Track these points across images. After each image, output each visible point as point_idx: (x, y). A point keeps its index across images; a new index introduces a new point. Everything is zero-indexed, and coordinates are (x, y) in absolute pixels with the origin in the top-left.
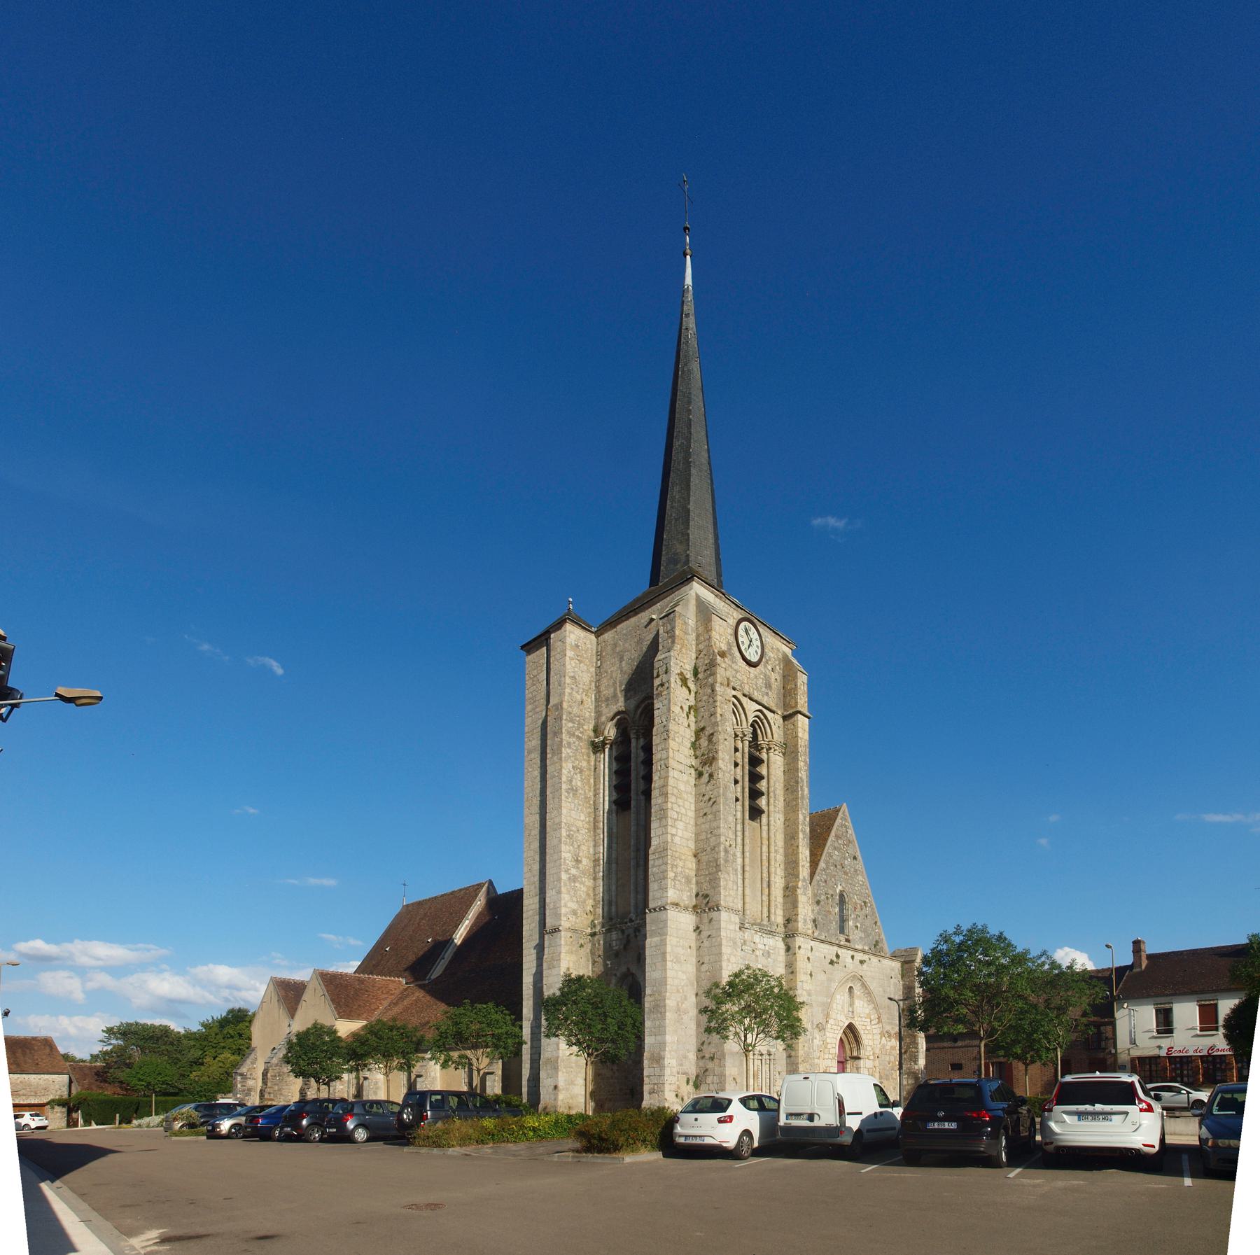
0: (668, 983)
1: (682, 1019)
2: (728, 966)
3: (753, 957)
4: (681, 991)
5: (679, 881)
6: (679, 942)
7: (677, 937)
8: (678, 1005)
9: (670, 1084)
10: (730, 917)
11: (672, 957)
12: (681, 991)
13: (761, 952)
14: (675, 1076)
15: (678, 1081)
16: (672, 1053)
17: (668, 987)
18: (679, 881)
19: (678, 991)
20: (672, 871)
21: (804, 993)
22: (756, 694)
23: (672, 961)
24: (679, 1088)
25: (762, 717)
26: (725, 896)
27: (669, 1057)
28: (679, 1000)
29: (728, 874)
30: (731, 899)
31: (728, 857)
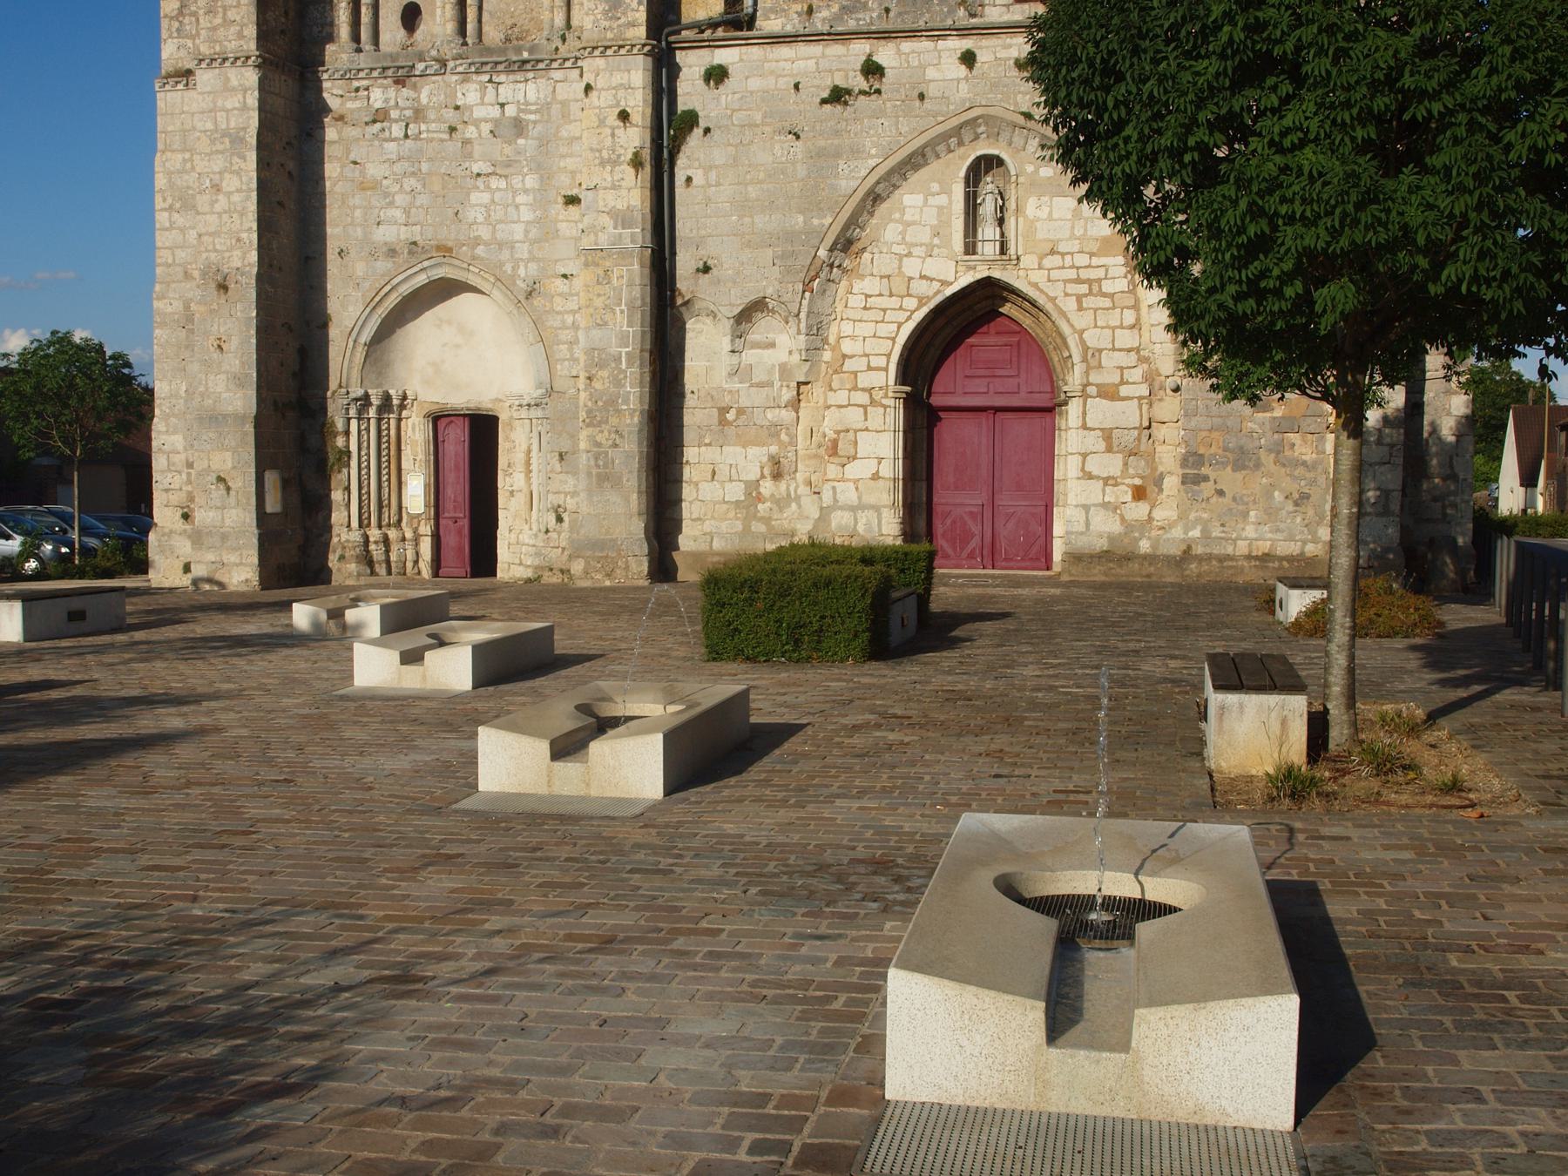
0: (159, 261)
2: (213, 203)
3: (453, 147)
7: (183, 151)
9: (167, 490)
10: (228, 79)
13: (486, 128)
14: (180, 472)
15: (189, 482)
16: (173, 420)
17: (159, 270)
19: (187, 276)
21: (606, 221)
23: (170, 209)
26: (214, 29)
27: (164, 429)
30: (234, 29)
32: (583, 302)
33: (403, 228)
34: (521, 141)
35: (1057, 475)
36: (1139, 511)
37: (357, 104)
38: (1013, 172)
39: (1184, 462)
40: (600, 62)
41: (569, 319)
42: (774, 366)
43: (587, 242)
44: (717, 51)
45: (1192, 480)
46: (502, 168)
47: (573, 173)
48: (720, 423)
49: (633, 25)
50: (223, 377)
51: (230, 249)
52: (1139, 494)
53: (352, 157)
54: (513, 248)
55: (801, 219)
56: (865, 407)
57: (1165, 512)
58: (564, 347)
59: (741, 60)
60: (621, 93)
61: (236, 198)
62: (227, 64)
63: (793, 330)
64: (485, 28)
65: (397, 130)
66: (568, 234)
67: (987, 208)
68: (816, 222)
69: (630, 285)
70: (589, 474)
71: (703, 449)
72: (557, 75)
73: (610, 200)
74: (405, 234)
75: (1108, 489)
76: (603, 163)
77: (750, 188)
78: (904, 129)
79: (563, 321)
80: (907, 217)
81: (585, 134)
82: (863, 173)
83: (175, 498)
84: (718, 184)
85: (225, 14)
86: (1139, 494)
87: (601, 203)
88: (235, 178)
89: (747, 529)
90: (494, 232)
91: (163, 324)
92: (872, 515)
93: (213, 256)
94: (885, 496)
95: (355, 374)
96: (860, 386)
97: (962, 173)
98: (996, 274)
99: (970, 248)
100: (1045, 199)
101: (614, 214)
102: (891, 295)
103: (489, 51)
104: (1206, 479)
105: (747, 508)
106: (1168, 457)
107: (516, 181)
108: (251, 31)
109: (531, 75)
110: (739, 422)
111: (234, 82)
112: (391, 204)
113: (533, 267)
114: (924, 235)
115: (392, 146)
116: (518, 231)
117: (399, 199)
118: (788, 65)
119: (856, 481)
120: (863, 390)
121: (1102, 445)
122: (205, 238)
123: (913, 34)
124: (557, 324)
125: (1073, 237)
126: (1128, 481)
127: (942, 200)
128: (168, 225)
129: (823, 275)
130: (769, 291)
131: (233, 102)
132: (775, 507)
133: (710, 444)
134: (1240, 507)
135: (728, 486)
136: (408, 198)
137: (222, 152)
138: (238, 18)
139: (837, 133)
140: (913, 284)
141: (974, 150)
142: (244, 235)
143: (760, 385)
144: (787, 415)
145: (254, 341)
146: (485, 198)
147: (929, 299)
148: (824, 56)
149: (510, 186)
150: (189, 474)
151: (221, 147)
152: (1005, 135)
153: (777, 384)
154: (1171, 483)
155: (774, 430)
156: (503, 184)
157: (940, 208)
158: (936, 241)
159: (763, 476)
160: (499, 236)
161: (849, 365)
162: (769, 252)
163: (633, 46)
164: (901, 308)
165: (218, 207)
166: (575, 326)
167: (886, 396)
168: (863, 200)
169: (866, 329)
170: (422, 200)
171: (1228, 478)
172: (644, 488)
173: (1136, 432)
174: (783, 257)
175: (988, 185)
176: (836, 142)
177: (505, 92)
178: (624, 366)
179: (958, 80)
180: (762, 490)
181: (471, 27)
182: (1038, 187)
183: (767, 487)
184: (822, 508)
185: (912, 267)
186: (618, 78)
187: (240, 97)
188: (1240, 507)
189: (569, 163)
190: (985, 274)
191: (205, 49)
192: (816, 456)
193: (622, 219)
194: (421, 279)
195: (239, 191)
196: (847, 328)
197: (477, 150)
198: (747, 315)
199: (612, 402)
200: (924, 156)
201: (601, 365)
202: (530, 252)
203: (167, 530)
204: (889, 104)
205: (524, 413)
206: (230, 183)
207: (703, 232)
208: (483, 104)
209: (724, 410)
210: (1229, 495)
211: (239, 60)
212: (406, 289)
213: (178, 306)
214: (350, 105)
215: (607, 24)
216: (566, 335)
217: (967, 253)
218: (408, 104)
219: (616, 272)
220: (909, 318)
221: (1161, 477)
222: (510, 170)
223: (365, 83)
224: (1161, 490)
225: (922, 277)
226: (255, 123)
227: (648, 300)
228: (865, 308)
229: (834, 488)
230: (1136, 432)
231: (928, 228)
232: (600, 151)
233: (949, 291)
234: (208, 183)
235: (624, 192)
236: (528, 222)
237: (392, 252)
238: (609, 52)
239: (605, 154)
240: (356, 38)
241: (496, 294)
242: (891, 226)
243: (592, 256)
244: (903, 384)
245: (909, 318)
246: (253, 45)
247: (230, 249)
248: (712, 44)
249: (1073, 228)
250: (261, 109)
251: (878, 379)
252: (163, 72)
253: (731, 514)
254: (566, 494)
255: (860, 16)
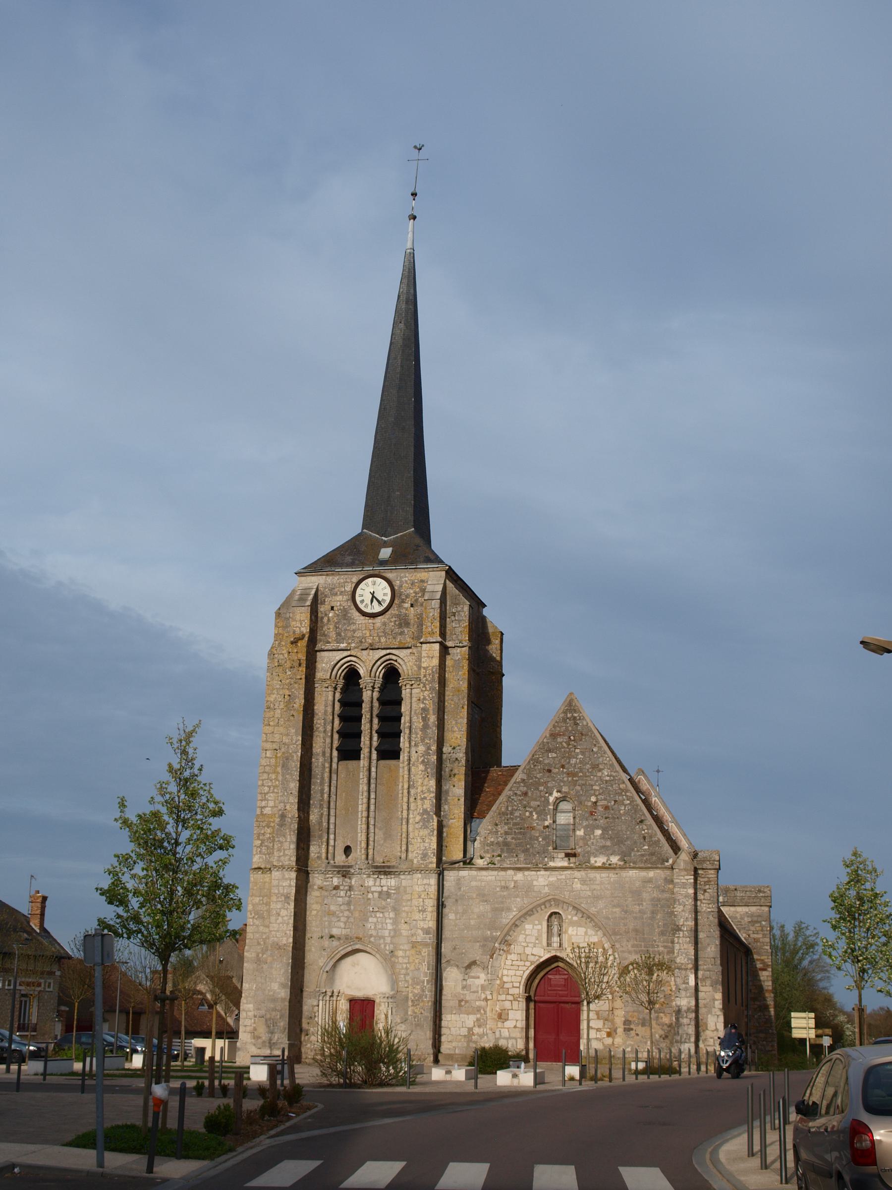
1: (262, 968)
4: (262, 943)
5: (266, 846)
6: (262, 900)
7: (259, 896)
8: (258, 956)
10: (284, 875)
11: (253, 915)
12: (262, 943)
14: (251, 1019)
15: (255, 1023)
16: (250, 999)
17: (247, 941)
18: (266, 846)
19: (259, 944)
20: (258, 839)
21: (420, 932)
22: (383, 640)
23: (253, 917)
24: (255, 1029)
25: (394, 658)
26: (279, 857)
28: (260, 951)
29: (284, 836)
30: (287, 857)
31: (285, 821)
32: (411, 960)
33: (343, 930)
34: (388, 900)
35: (581, 1028)
36: (609, 1041)
37: (328, 883)
38: (564, 918)
39: (625, 1023)
40: (419, 875)
41: (405, 966)
42: (479, 985)
43: (414, 939)
44: (461, 872)
45: (627, 1030)
46: (382, 909)
47: (407, 913)
48: (459, 1006)
49: (431, 863)
50: (277, 984)
51: (282, 937)
52: (609, 1035)
53: (325, 902)
54: (384, 939)
55: (489, 932)
56: (511, 1001)
57: (618, 1040)
58: (402, 976)
59: (469, 875)
60: (426, 886)
61: (286, 918)
62: (284, 870)
63: (487, 972)
64: (375, 857)
65: (342, 893)
66: (405, 934)
67: (555, 929)
68: (494, 934)
69: (429, 955)
70: (412, 1024)
71: (453, 1015)
72: (402, 877)
73: (422, 924)
74: (344, 932)
75: (598, 1033)
76: (419, 911)
77: (471, 921)
78: (526, 902)
79: (402, 967)
80: (527, 933)
81: (414, 901)
82: (511, 917)
83: (248, 1029)
84: (460, 919)
85: (284, 851)
86: (609, 1035)
87: (419, 925)
88: (286, 911)
89: (468, 1045)
90: (378, 933)
91: (248, 962)
92: (514, 1041)
93: (275, 938)
94: (519, 1034)
95: (323, 984)
96: (510, 993)
97: (546, 918)
98: (558, 954)
99: (549, 945)
100: (575, 928)
101: (422, 929)
102: (521, 961)
103: (377, 867)
104: (632, 1029)
105: (468, 1038)
106: (619, 1021)
107: (386, 914)
108: (294, 859)
109: (393, 876)
110: (466, 1006)
111: (287, 876)
112: (339, 921)
113: (392, 946)
114: (533, 940)
115: (340, 899)
116: (386, 933)
117: (343, 919)
118: (485, 878)
119: (508, 1028)
120: (511, 995)
121: (595, 1017)
122: (273, 933)
123: (528, 869)
124: (400, 967)
125: (584, 942)
126: (605, 1030)
127: (539, 927)
128: (252, 924)
129: (496, 953)
130: (478, 958)
131: (285, 884)
132: (479, 1038)
133: (455, 1014)
134: (645, 1040)
135: (462, 1029)
136: (346, 919)
137: (282, 901)
138: (289, 854)
139: (502, 903)
140: (529, 957)
141: (550, 910)
142: (288, 932)
143: (474, 992)
144: (483, 1003)
145: (290, 971)
146: (375, 920)
147: (534, 962)
148: (498, 875)
149: (384, 916)
150: (255, 1020)
151: (281, 900)
152: (561, 905)
153: (480, 992)
154: (620, 1030)
155: (478, 1009)
156: (381, 915)
157: (538, 930)
158: (537, 942)
159: (474, 1026)
160: (380, 934)
161: (506, 986)
162: (478, 944)
163: (431, 870)
164: (524, 966)
165: (278, 922)
166: (407, 969)
167: (519, 997)
168: (511, 927)
169: (512, 973)
170: (352, 920)
171: (640, 1030)
172: (432, 1029)
173: (607, 1012)
174: (484, 946)
175: (555, 922)
176: (502, 906)
177: (384, 882)
178: (425, 984)
179: (544, 886)
180: (474, 1031)
181: (370, 857)
182: (572, 924)
183: (476, 1030)
184: (496, 1038)
185: (528, 951)
186: (425, 881)
187: (289, 882)
188: (645, 1040)
189: (406, 909)
190: (554, 954)
191: (275, 863)
192: (494, 1019)
193: (427, 932)
194: (350, 949)
195: (287, 916)
196: (505, 972)
197: (372, 902)
198: (469, 966)
199: (421, 997)
200: (532, 911)
201: (418, 984)
202: (391, 941)
203: (244, 1042)
204: (520, 893)
205: (385, 1000)
206: (283, 913)
207: (454, 936)
208: (375, 885)
209: (460, 1001)
210: (640, 1036)
211: (290, 868)
212: (343, 953)
213: (254, 955)
214: (325, 883)
215: (422, 862)
216: (403, 971)
217: (548, 946)
218: (347, 884)
219: (424, 950)
220: (527, 969)
221: (617, 1028)
222: (384, 910)
223: (331, 876)
224: (616, 1034)
225: (532, 955)
226: (294, 891)
227: (435, 961)
228: (512, 965)
229: (500, 1031)
230: (607, 1012)
231: (534, 937)
232: (418, 907)
233: (541, 960)
234: (275, 912)
235: (427, 922)
236: (390, 930)
237: (339, 939)
238: (423, 872)
239: (420, 908)
240: (327, 858)
241: (378, 956)
242: (521, 936)
243: (414, 945)
244: (525, 993)
245: (527, 969)
246: (294, 864)
247: (282, 937)
248: (459, 869)
249: (585, 938)
250: (296, 886)
251: (516, 991)
252: (253, 867)
253: (463, 1040)
254: (402, 1031)
255: (511, 859)
